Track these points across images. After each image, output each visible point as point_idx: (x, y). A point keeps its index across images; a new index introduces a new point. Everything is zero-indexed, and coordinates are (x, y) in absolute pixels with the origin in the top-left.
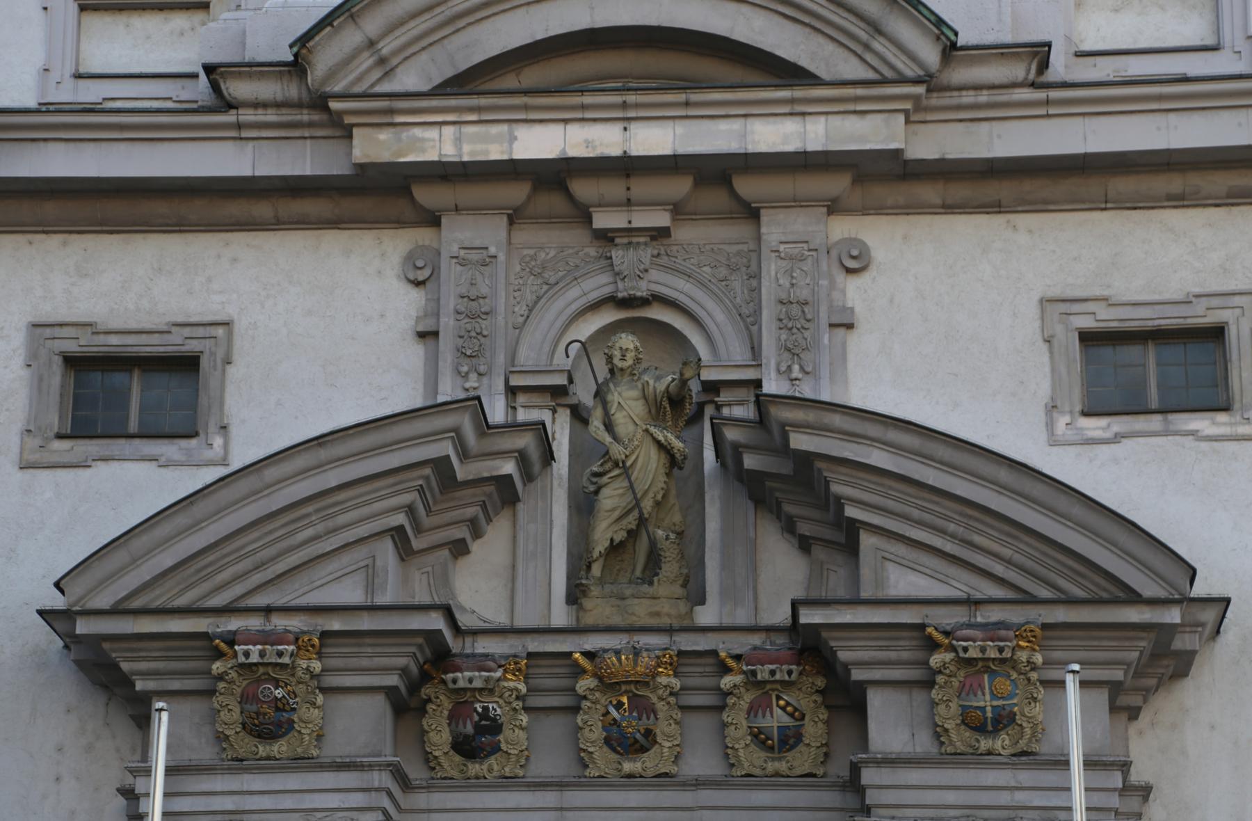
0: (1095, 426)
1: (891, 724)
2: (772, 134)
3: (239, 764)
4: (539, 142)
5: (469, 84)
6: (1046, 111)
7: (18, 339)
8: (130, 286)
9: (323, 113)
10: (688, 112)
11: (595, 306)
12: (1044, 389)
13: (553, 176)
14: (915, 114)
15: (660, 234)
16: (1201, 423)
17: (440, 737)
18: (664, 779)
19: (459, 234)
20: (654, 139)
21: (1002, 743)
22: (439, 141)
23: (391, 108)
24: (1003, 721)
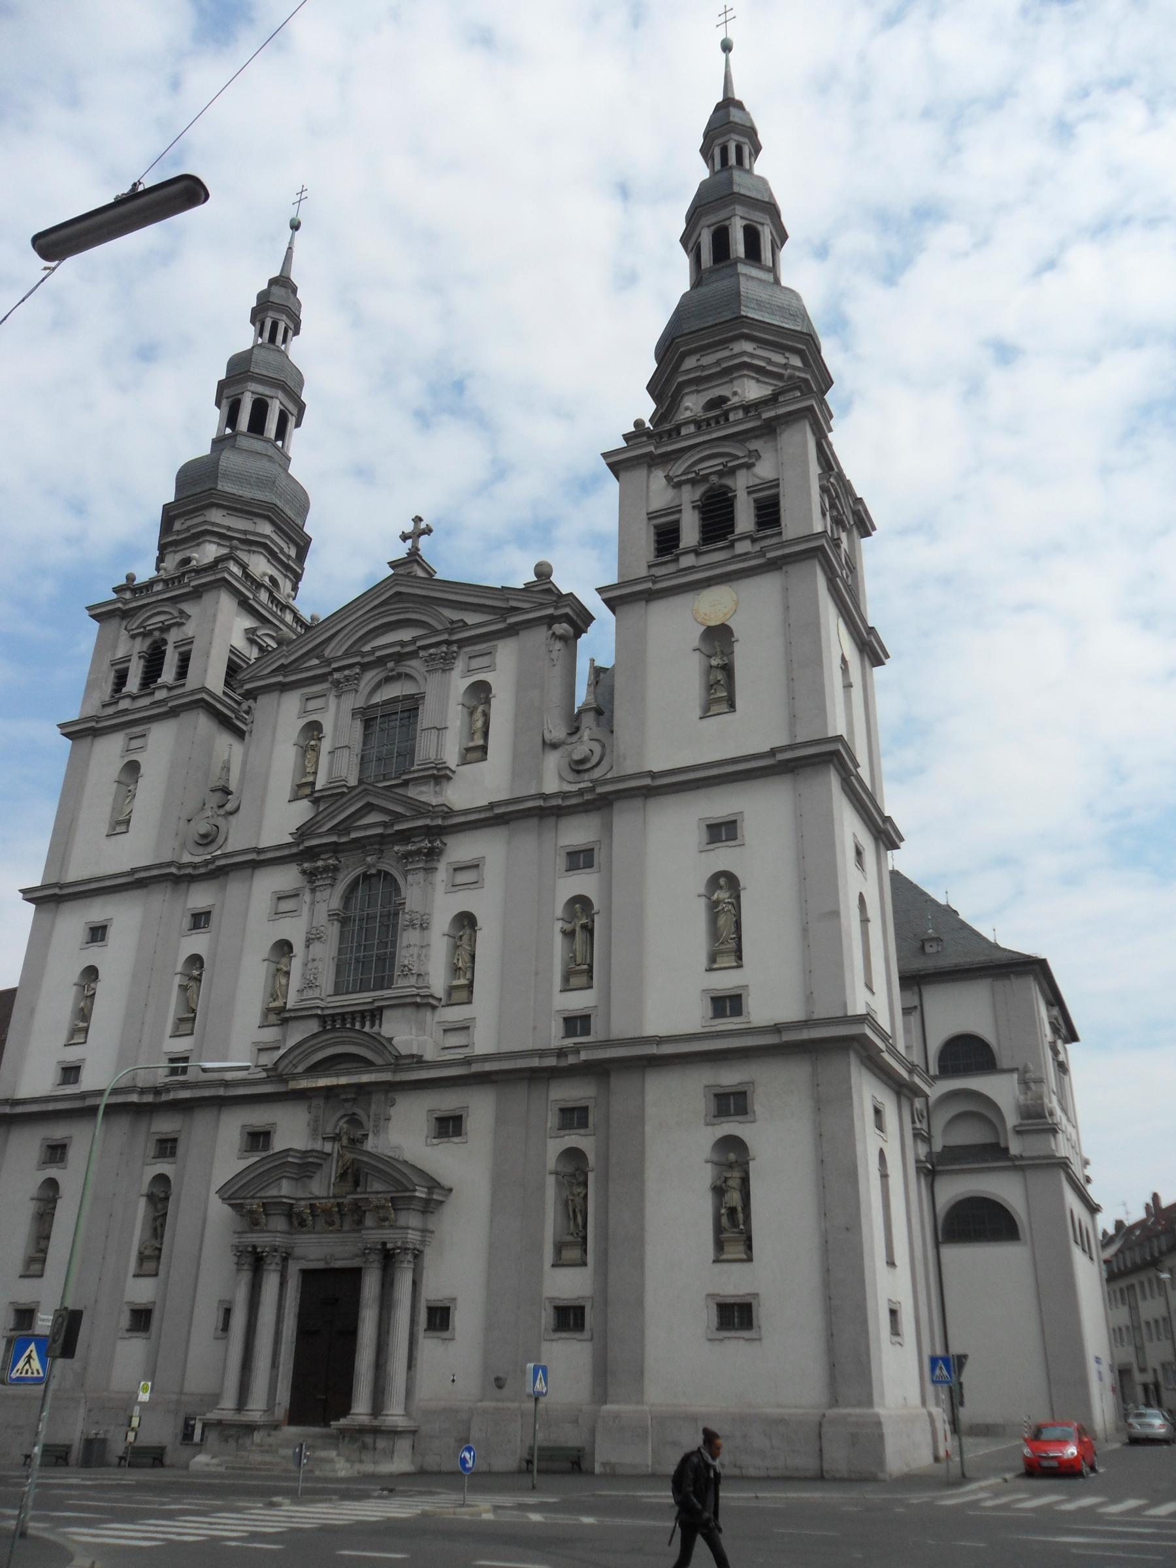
0: (435, 1141)
1: (369, 1221)
2: (365, 1078)
3: (252, 1231)
4: (322, 1082)
5: (315, 1069)
6: (422, 1068)
7: (239, 1130)
8: (258, 1117)
9: (282, 1079)
10: (348, 1073)
11: (345, 1116)
12: (425, 1132)
13: (329, 1089)
14: (395, 1072)
15: (354, 1099)
16: (455, 1139)
17: (296, 1223)
18: (339, 1231)
19: (315, 1102)
20: (343, 1080)
21: (386, 1224)
22: (304, 1084)
23: (295, 1077)
24: (385, 1219)
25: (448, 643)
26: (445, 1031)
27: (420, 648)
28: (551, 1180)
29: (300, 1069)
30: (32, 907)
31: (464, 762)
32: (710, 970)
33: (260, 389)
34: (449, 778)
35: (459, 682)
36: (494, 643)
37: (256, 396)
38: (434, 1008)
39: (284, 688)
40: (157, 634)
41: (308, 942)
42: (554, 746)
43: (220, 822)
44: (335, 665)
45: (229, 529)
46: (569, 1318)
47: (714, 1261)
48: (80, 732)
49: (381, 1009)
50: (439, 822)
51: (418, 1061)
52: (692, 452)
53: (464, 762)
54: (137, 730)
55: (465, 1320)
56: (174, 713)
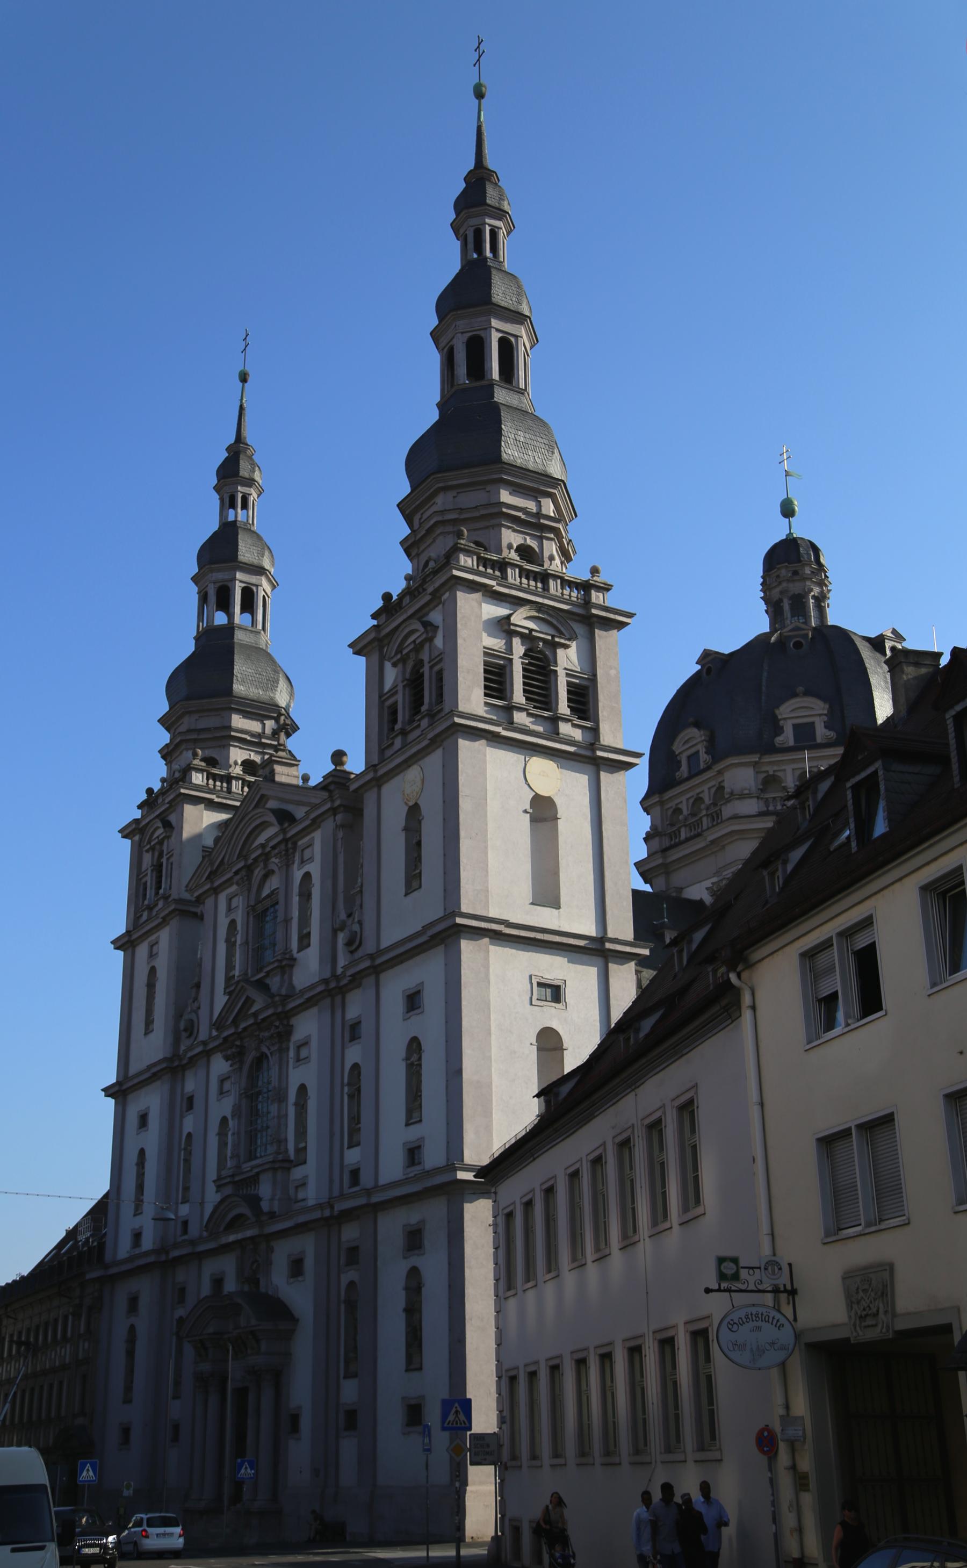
0: (292, 1280)
4: (232, 1238)
25: (285, 841)
26: (297, 1187)
27: (273, 848)
28: (343, 1307)
29: (222, 1229)
30: (111, 1102)
31: (300, 949)
32: (407, 1125)
33: (220, 576)
34: (292, 966)
35: (298, 875)
36: (312, 835)
37: (218, 585)
38: (289, 1169)
39: (216, 891)
40: (158, 847)
41: (232, 1116)
42: (342, 929)
43: (194, 1017)
44: (234, 870)
45: (200, 731)
46: (351, 1419)
47: (406, 1371)
48: (125, 943)
49: (258, 1174)
50: (280, 1009)
51: (272, 1215)
52: (397, 633)
53: (300, 949)
54: (153, 938)
55: (306, 1423)
56: (165, 921)
